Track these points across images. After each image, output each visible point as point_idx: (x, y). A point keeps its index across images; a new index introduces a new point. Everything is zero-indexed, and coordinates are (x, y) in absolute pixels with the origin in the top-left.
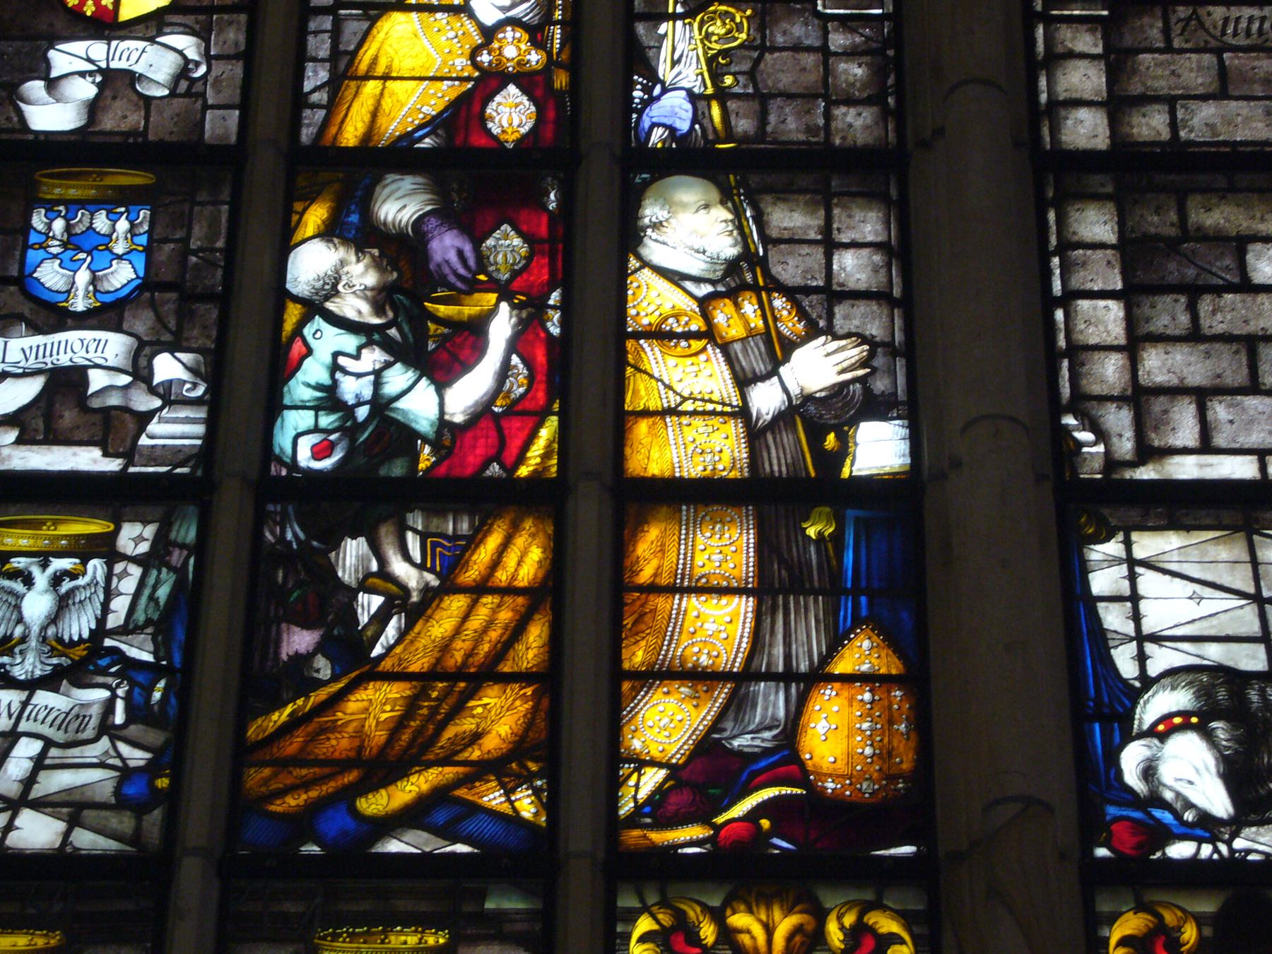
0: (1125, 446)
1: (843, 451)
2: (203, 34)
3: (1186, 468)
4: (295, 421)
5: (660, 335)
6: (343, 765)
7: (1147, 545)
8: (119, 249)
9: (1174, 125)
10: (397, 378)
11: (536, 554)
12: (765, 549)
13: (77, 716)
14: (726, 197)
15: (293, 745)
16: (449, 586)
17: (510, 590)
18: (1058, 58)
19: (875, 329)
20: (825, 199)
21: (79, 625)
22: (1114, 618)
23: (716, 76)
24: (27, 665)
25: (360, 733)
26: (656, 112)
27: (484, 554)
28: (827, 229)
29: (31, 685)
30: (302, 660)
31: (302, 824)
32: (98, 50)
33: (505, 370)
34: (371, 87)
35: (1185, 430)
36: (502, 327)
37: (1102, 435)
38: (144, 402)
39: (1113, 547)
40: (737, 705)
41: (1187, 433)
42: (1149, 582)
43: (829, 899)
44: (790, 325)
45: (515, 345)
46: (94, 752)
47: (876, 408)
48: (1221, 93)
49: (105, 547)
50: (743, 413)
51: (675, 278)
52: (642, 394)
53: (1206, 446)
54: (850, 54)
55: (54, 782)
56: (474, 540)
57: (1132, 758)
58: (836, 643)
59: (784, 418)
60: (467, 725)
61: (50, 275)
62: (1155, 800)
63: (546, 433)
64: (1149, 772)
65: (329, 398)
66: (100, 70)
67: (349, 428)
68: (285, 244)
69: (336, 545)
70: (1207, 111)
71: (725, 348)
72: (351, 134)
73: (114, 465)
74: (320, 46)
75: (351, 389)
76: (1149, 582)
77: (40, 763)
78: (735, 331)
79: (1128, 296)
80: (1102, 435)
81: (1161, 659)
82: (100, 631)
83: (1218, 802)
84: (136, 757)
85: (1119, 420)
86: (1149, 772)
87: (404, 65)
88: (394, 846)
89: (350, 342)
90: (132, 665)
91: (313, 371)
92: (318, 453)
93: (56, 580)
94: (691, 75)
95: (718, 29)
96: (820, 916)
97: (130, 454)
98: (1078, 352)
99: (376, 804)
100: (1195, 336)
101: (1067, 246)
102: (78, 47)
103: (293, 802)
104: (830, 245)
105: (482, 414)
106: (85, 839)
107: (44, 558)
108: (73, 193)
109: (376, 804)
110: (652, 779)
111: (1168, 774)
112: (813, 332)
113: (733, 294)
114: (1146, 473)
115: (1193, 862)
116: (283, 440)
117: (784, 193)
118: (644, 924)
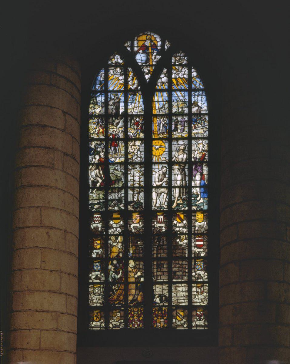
0: (156, 279)
1: (140, 280)
2: (102, 249)
3: (159, 281)
4: (110, 278)
5: (130, 272)
6: (114, 301)
7: (157, 286)
8: (99, 266)
9: (160, 255)
10: (115, 275)
11: (123, 287)
12: (136, 287)
13: (100, 298)
14: (134, 261)
15: (111, 299)
16: (119, 289)
17: (122, 289)
18: (154, 250)
19: (142, 271)
20: (139, 262)
21: (99, 292)
22: (155, 291)
23: (133, 252)
24: (97, 295)
25: (115, 299)
26: (130, 255)
27: (121, 287)
28: (140, 264)
29: (97, 296)
30: (111, 294)
31: (112, 304)
32: (96, 251)
33: (121, 275)
34: (113, 253)
35: (159, 278)
36: (121, 272)
37: (155, 278)
38: (101, 277)
39: (155, 286)
40: (134, 297)
41: (159, 278)
42: (157, 288)
43: (139, 308)
44: (137, 271)
45: (122, 273)
46: (101, 300)
47: (142, 277)
48: (163, 253)
49: (100, 287)
50: (135, 277)
51: (131, 267)
52: (129, 276)
53: (160, 279)
54: (141, 250)
55: (99, 302)
56: (120, 286)
57: (155, 299)
58: (140, 293)
59: (137, 277)
60: (120, 298)
61: (95, 268)
62: (156, 302)
63: (124, 279)
64: (156, 300)
65: (111, 277)
66: (97, 252)
67: (113, 278)
68: (108, 266)
69: (112, 286)
70: (162, 254)
71: (134, 273)
72: (112, 257)
73: (100, 281)
74: (109, 250)
75: (113, 276)
76: (157, 288)
77: (98, 301)
78: (134, 271)
79: (157, 269)
80: (155, 278)
81: (157, 293)
82: (100, 292)
83: (159, 302)
84: (103, 300)
85: (156, 277)
86: (156, 300)
87: (114, 251)
88: (117, 305)
89: (112, 272)
90: (102, 295)
91: (111, 275)
92: (111, 280)
93: (98, 289)
94: (131, 252)
95: (133, 248)
96: (138, 309)
97: (101, 281)
98: (154, 273)
99: (116, 303)
100: (160, 271)
101: (154, 265)
102: (95, 250)
103: (111, 303)
104: (140, 265)
105: (120, 277)
106: (101, 305)
107: (97, 288)
108: (96, 262)
109: (116, 303)
110: (130, 301)
111: (157, 300)
112: (139, 271)
113: (134, 269)
114: (157, 281)
115: (158, 306)
116: (109, 279)
117: (137, 261)
118: (130, 310)
